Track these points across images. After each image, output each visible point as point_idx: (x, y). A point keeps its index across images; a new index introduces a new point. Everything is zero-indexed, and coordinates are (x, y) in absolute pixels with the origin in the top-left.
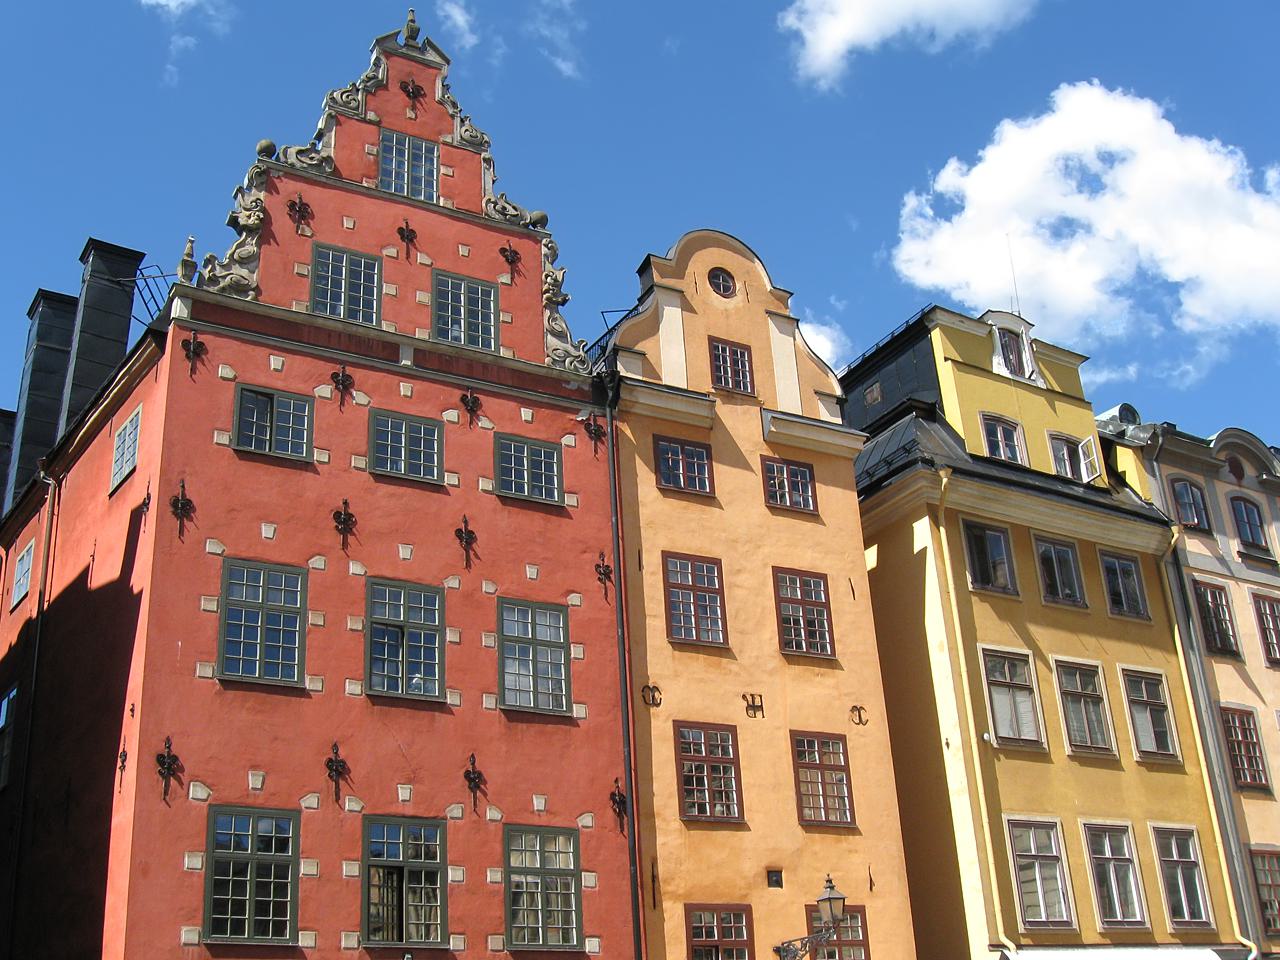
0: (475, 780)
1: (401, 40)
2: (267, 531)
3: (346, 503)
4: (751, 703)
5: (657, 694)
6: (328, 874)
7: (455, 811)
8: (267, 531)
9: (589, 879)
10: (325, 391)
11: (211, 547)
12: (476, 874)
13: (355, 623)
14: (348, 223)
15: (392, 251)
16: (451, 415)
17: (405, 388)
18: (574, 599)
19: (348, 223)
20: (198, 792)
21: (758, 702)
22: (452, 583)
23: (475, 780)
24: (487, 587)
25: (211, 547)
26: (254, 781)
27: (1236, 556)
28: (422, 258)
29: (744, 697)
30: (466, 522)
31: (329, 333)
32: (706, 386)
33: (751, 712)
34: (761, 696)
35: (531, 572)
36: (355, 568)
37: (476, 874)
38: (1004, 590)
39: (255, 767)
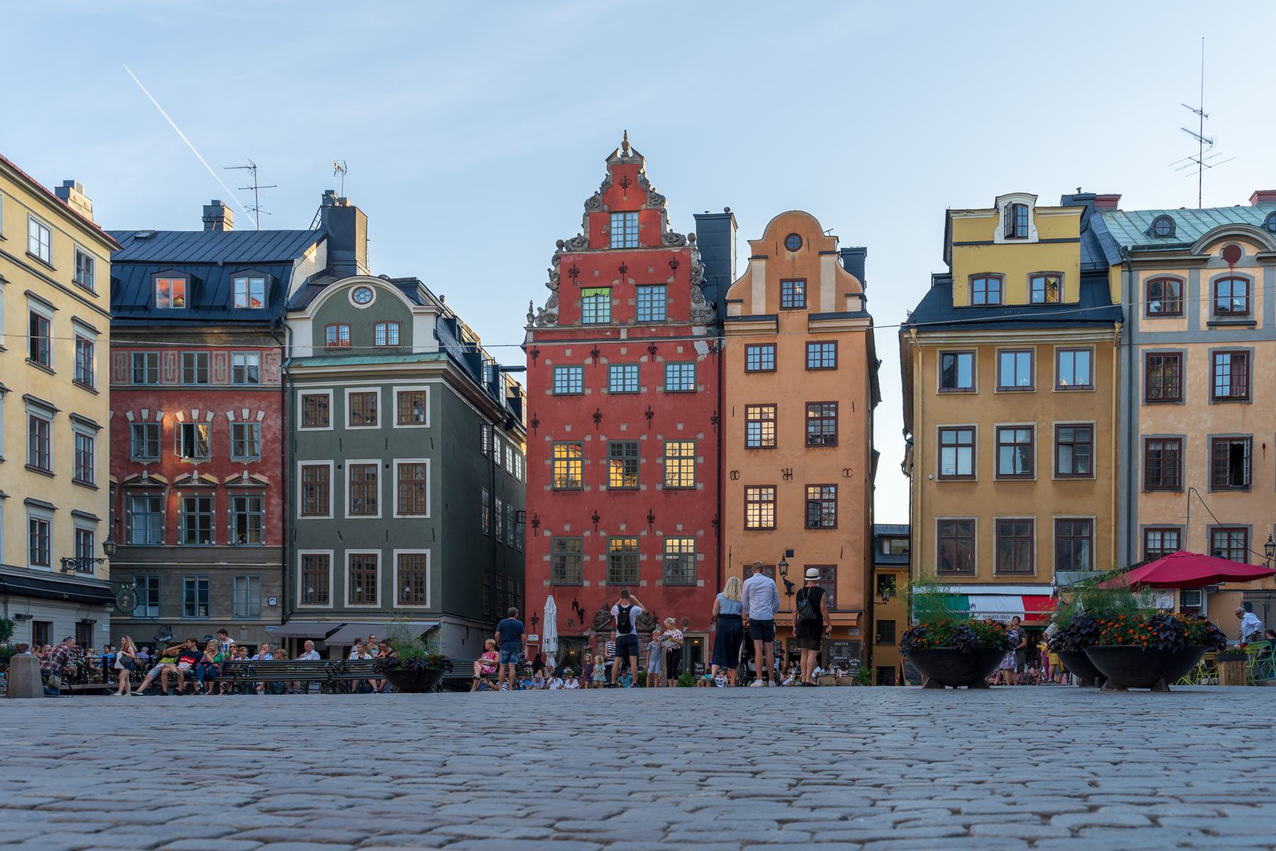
0: (651, 519)
2: (568, 428)
6: (595, 559)
7: (644, 533)
10: (589, 361)
11: (548, 439)
12: (651, 556)
14: (597, 273)
15: (616, 282)
16: (644, 359)
19: (597, 273)
20: (547, 533)
22: (644, 437)
23: (651, 519)
25: (548, 439)
27: (1204, 327)
28: (631, 281)
31: (589, 332)
35: (680, 427)
37: (651, 556)
38: (965, 390)
39: (567, 522)
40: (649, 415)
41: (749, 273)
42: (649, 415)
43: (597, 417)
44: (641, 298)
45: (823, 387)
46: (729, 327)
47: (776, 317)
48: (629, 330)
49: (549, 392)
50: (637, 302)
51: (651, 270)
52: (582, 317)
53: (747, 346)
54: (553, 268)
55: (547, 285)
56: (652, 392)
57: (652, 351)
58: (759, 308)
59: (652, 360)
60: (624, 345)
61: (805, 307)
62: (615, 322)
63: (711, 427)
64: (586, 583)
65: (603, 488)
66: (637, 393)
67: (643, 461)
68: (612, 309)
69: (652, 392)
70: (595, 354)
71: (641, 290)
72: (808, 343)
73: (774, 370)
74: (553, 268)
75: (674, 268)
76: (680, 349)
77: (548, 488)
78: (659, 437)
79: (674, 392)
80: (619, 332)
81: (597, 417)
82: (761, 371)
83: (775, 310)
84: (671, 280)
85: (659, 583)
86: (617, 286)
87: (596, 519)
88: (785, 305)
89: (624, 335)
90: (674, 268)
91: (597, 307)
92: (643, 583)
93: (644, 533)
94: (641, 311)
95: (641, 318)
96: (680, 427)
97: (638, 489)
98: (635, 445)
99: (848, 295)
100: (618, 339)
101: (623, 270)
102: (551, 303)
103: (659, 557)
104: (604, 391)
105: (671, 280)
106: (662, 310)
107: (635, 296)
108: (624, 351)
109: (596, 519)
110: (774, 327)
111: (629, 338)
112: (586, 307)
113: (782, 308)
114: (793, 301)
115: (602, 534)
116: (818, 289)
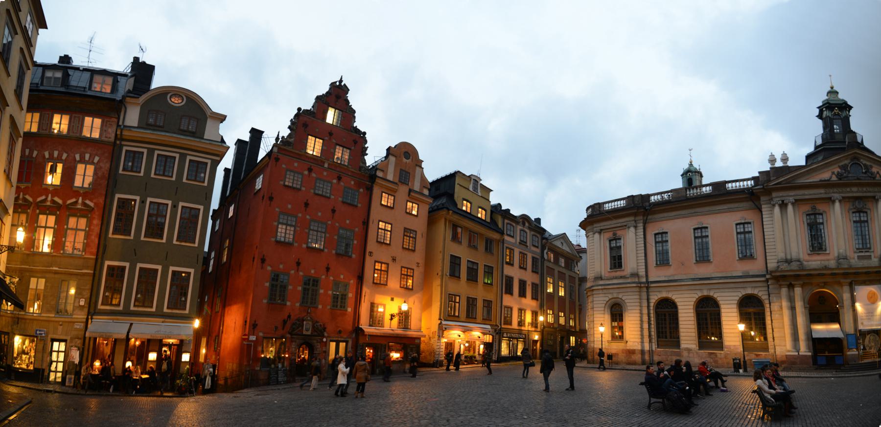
0: (328, 269)
2: (290, 206)
8: (290, 206)
9: (350, 295)
11: (277, 209)
20: (269, 268)
23: (328, 269)
26: (281, 266)
32: (397, 181)
35: (348, 222)
40: (334, 211)
42: (334, 211)
46: (378, 180)
49: (282, 183)
57: (339, 179)
58: (390, 177)
64: (288, 303)
65: (304, 246)
66: (329, 198)
67: (328, 235)
73: (393, 208)
76: (353, 183)
77: (273, 239)
79: (349, 204)
82: (387, 206)
83: (397, 181)
85: (329, 307)
87: (298, 264)
92: (320, 307)
93: (323, 277)
96: (348, 222)
102: (289, 136)
103: (330, 292)
104: (312, 191)
107: (335, 149)
108: (325, 174)
109: (298, 264)
115: (301, 273)
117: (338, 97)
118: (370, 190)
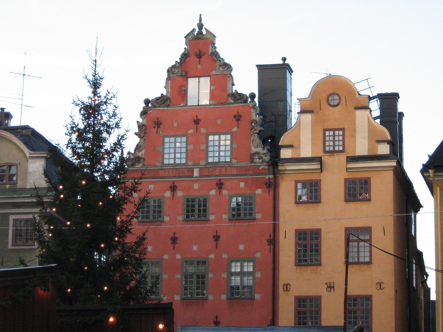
1: (197, 30)
3: (175, 234)
4: (329, 286)
5: (289, 287)
10: (168, 194)
13: (178, 276)
14: (175, 124)
15: (191, 131)
17: (196, 186)
18: (258, 255)
19: (175, 124)
21: (332, 285)
22: (212, 256)
24: (225, 256)
29: (326, 284)
30: (217, 232)
33: (329, 289)
34: (334, 283)
35: (242, 247)
36: (178, 257)
41: (298, 123)
42: (217, 238)
43: (174, 240)
44: (211, 144)
45: (358, 214)
47: (319, 160)
48: (200, 169)
50: (207, 146)
51: (219, 122)
52: (163, 159)
53: (297, 182)
54: (141, 121)
55: (136, 134)
56: (219, 219)
57: (220, 186)
58: (306, 151)
59: (220, 193)
60: (196, 181)
61: (343, 151)
62: (190, 163)
63: (267, 247)
68: (187, 152)
69: (219, 219)
70: (173, 189)
71: (211, 138)
72: (346, 180)
74: (141, 121)
75: (238, 120)
76: (242, 185)
78: (225, 256)
80: (192, 171)
81: (174, 240)
83: (319, 153)
84: (235, 129)
86: (191, 134)
88: (327, 149)
89: (196, 173)
90: (238, 120)
91: (175, 151)
94: (210, 154)
95: (210, 160)
96: (242, 247)
97: (207, 299)
98: (204, 263)
99: (379, 142)
100: (192, 176)
101: (197, 122)
105: (235, 129)
106: (228, 153)
110: (318, 167)
111: (201, 176)
112: (166, 151)
113: (325, 152)
114: (334, 146)
116: (354, 136)
117: (199, 55)
118: (273, 186)
